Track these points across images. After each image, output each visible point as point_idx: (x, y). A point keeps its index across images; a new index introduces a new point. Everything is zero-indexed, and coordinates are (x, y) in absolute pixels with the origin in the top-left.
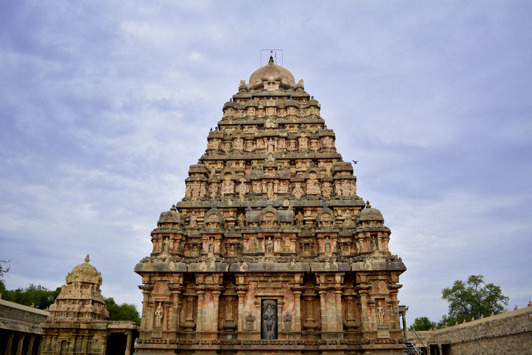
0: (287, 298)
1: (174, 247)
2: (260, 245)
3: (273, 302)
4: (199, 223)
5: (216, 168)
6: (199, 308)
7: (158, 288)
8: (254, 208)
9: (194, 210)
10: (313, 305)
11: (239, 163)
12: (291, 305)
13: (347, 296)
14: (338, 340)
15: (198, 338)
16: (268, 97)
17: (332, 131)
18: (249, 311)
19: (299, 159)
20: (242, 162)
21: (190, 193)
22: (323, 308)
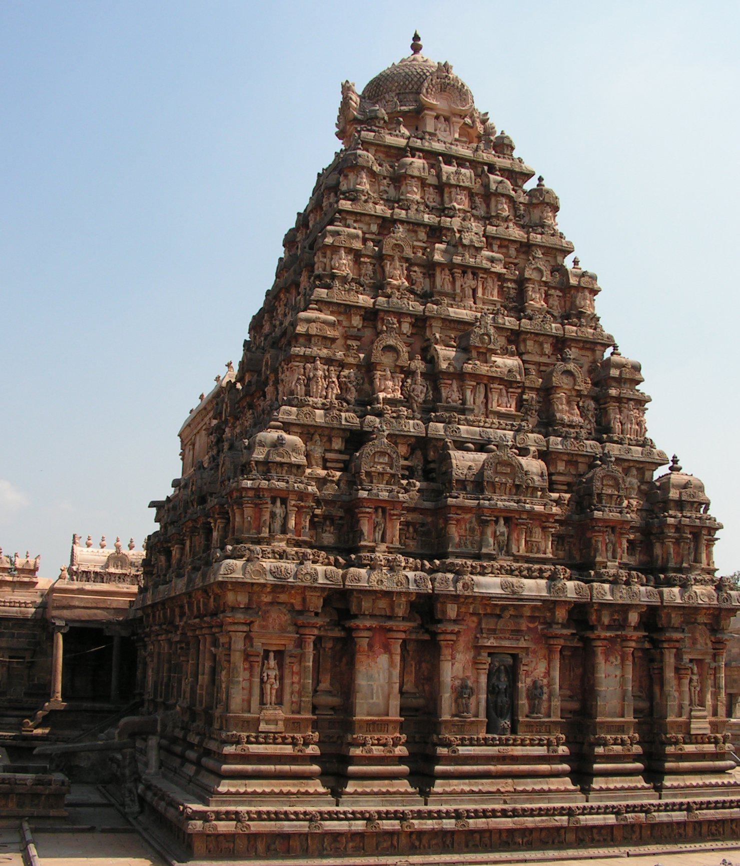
0: (534, 652)
2: (483, 533)
3: (510, 660)
4: (329, 465)
5: (345, 323)
7: (264, 619)
8: (461, 445)
9: (320, 431)
12: (542, 667)
14: (625, 737)
15: (359, 736)
18: (461, 675)
19: (532, 333)
20: (409, 320)
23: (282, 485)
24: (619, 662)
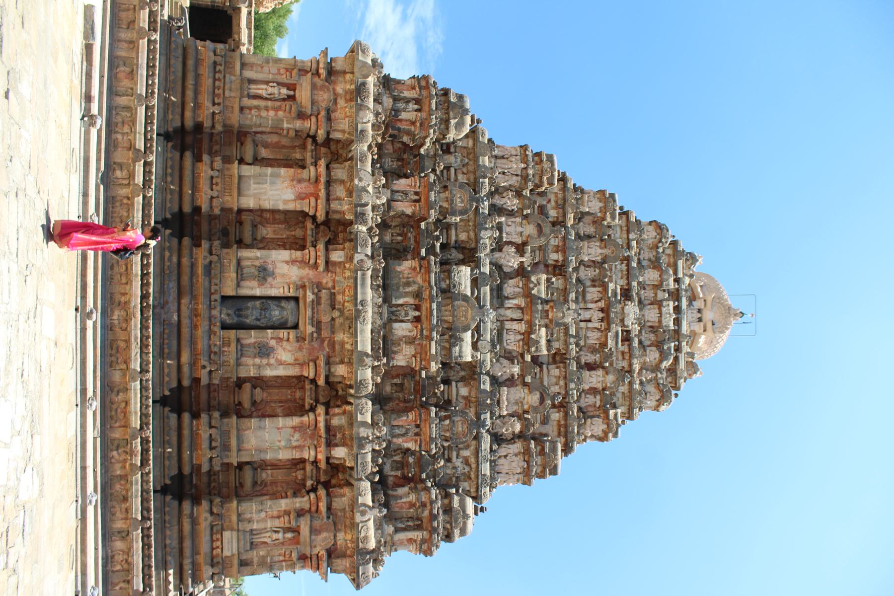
0: (300, 349)
1: (401, 120)
6: (283, 171)
8: (475, 283)
10: (286, 401)
11: (557, 252)
13: (304, 469)
16: (677, 309)
17: (616, 435)
18: (277, 271)
20: (561, 259)
21: (501, 154)
22: (281, 421)
23: (434, 106)
24: (295, 444)
